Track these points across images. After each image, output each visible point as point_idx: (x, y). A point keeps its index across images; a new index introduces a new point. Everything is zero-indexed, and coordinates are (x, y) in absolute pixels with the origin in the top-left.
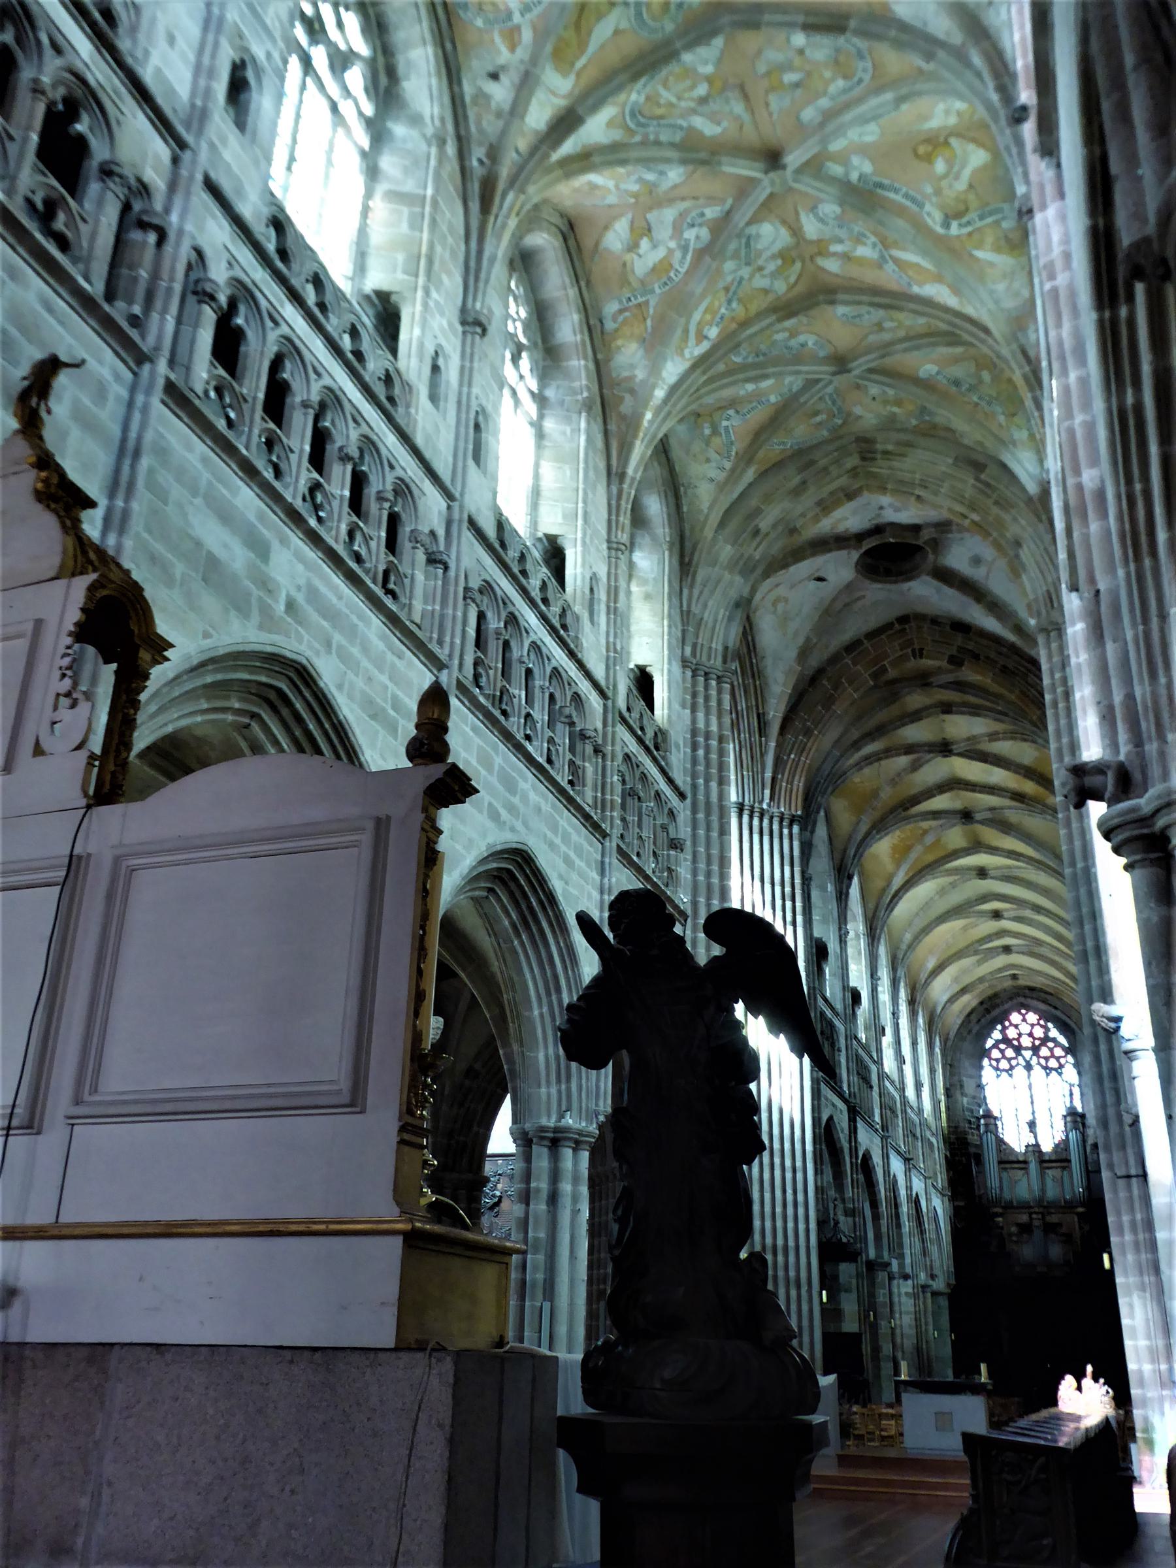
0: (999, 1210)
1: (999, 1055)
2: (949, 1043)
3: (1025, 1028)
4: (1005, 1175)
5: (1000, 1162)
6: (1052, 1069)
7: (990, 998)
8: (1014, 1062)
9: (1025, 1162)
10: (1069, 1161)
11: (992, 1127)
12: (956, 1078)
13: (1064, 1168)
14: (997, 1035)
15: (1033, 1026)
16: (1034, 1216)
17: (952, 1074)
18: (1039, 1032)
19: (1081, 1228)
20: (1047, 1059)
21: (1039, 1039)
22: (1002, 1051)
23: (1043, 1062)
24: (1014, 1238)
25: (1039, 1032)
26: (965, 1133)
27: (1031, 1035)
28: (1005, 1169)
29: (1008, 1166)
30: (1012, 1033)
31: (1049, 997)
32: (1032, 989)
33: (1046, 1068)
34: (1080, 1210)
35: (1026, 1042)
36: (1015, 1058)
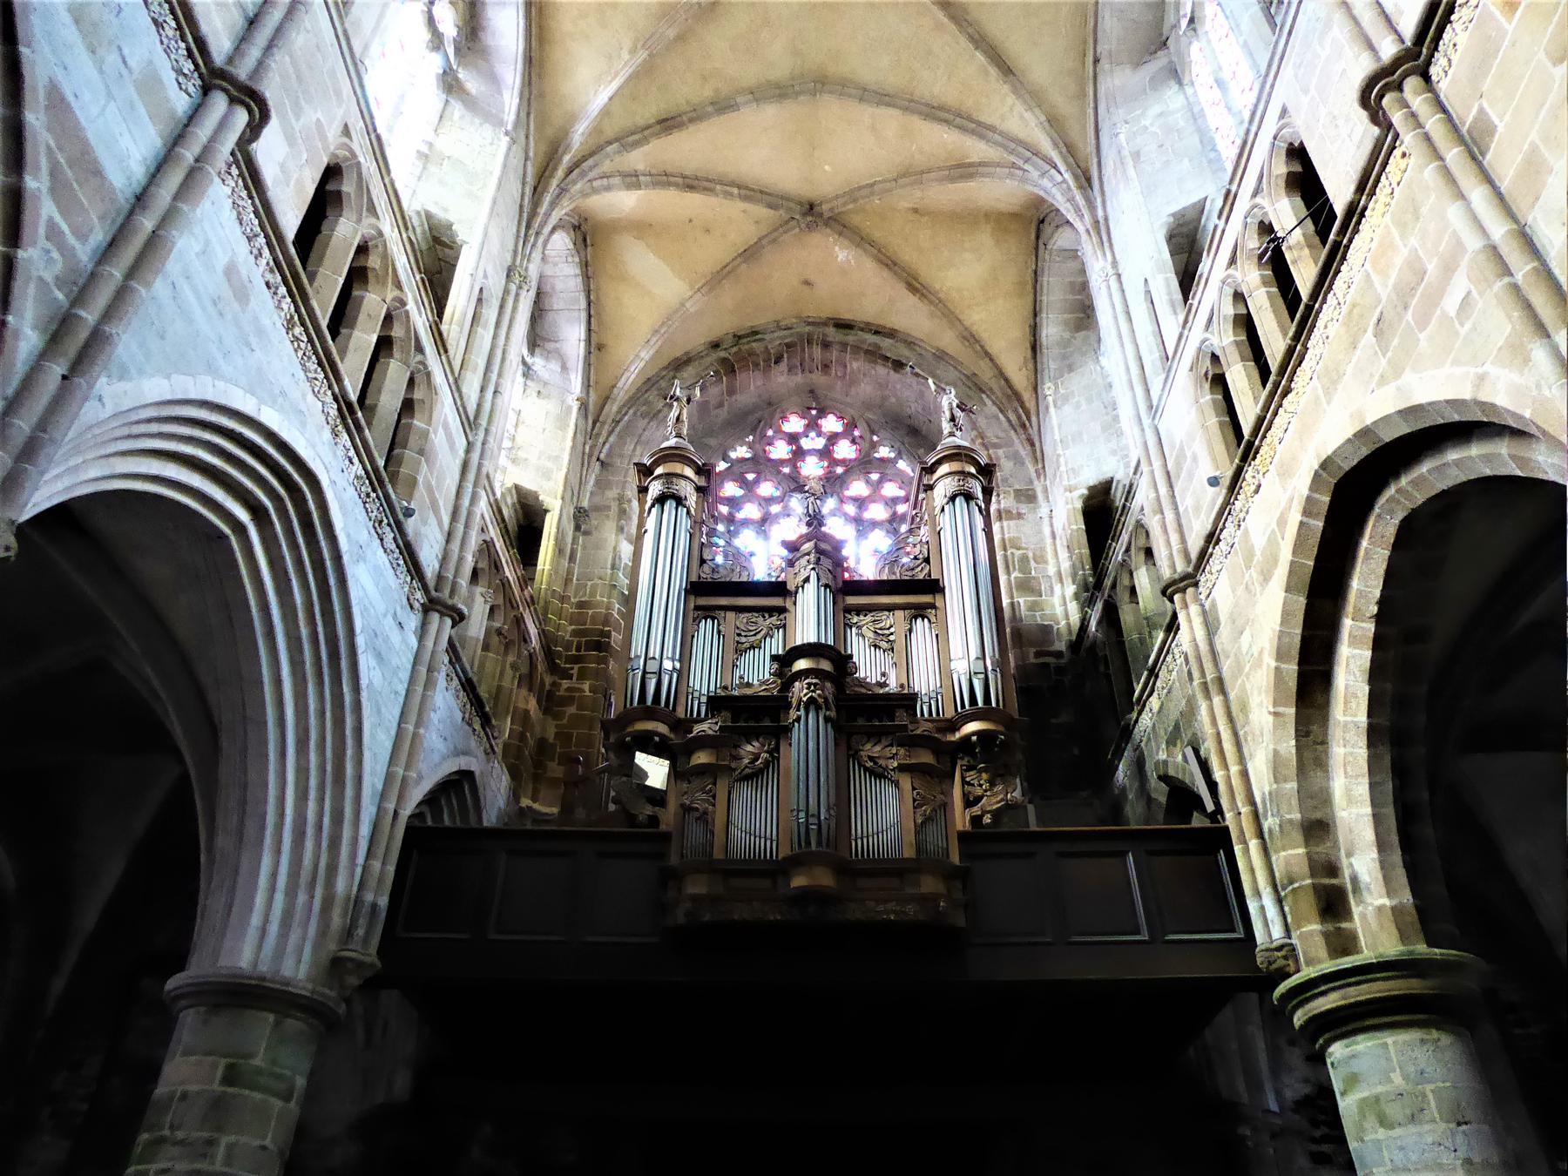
0: (662, 728)
1: (739, 492)
2: (612, 409)
3: (812, 442)
4: (706, 627)
5: (695, 588)
6: (874, 524)
7: (738, 338)
8: (775, 509)
9: (778, 589)
10: (934, 587)
11: (687, 490)
12: (612, 493)
13: (919, 612)
14: (741, 452)
15: (833, 438)
16: (802, 664)
17: (601, 484)
18: (845, 450)
19: (969, 802)
20: (861, 502)
21: (843, 462)
22: (749, 487)
23: (850, 509)
24: (701, 758)
25: (845, 450)
26: (607, 620)
27: (826, 453)
28: (708, 612)
29: (724, 601)
30: (780, 450)
31: (886, 343)
32: (844, 325)
33: (857, 521)
34: (972, 727)
35: (812, 468)
36: (781, 500)
